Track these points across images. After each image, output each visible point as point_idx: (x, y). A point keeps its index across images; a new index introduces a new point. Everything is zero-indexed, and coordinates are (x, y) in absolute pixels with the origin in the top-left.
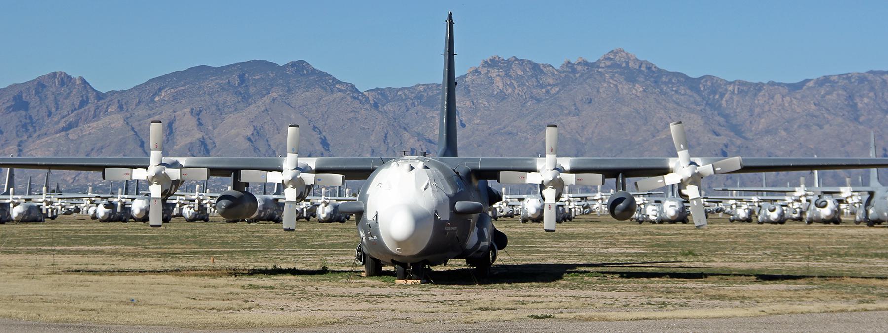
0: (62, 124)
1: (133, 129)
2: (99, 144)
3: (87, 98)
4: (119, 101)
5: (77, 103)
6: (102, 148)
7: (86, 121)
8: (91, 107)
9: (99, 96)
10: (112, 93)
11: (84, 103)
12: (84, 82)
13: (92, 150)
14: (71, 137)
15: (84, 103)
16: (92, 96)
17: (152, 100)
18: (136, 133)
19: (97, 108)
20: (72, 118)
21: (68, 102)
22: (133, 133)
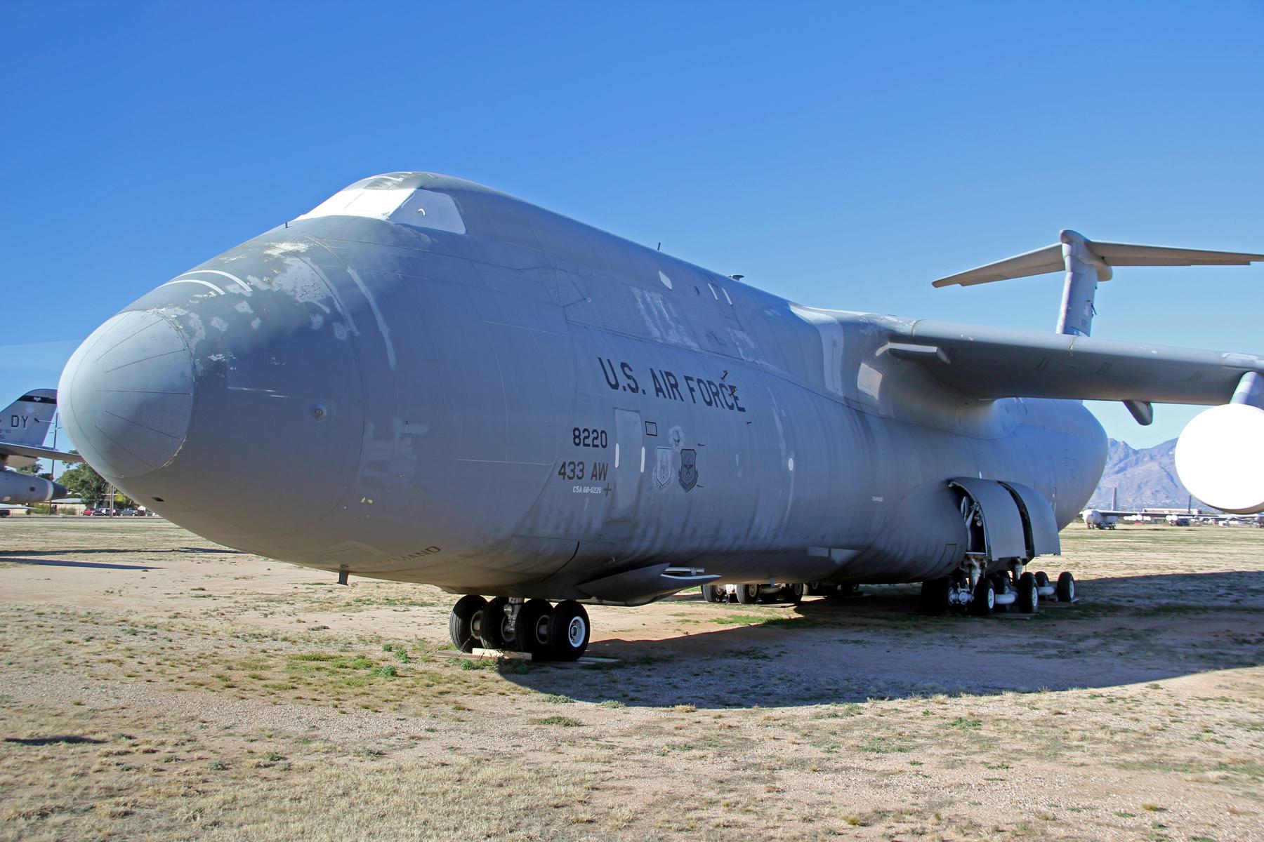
0: (1116, 469)
1: (1165, 471)
2: (1145, 480)
3: (1128, 453)
4: (1150, 455)
5: (1122, 456)
6: (1147, 482)
7: (1131, 466)
8: (1133, 458)
9: (1135, 452)
10: (1142, 450)
11: (1126, 456)
12: (1126, 444)
13: (1141, 483)
14: (1128, 475)
15: (1126, 456)
16: (1130, 451)
17: (1168, 454)
18: (1168, 473)
19: (1137, 459)
20: (1122, 465)
21: (1116, 456)
22: (1165, 473)
